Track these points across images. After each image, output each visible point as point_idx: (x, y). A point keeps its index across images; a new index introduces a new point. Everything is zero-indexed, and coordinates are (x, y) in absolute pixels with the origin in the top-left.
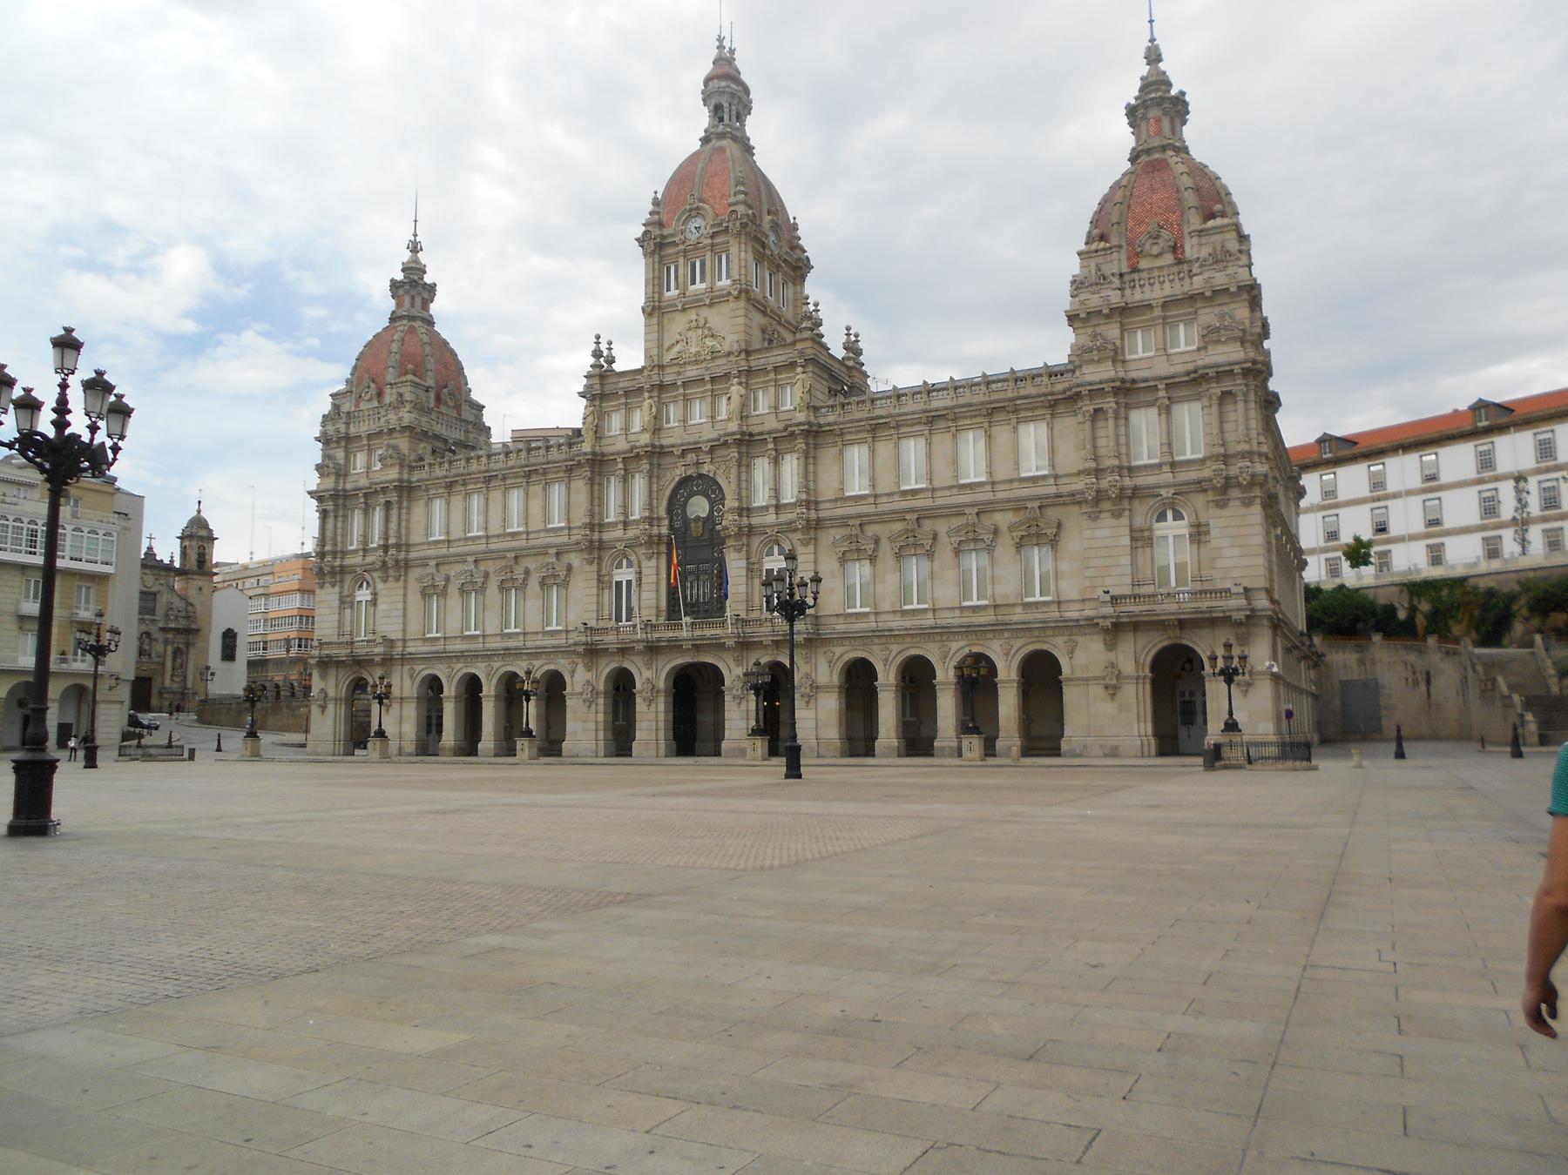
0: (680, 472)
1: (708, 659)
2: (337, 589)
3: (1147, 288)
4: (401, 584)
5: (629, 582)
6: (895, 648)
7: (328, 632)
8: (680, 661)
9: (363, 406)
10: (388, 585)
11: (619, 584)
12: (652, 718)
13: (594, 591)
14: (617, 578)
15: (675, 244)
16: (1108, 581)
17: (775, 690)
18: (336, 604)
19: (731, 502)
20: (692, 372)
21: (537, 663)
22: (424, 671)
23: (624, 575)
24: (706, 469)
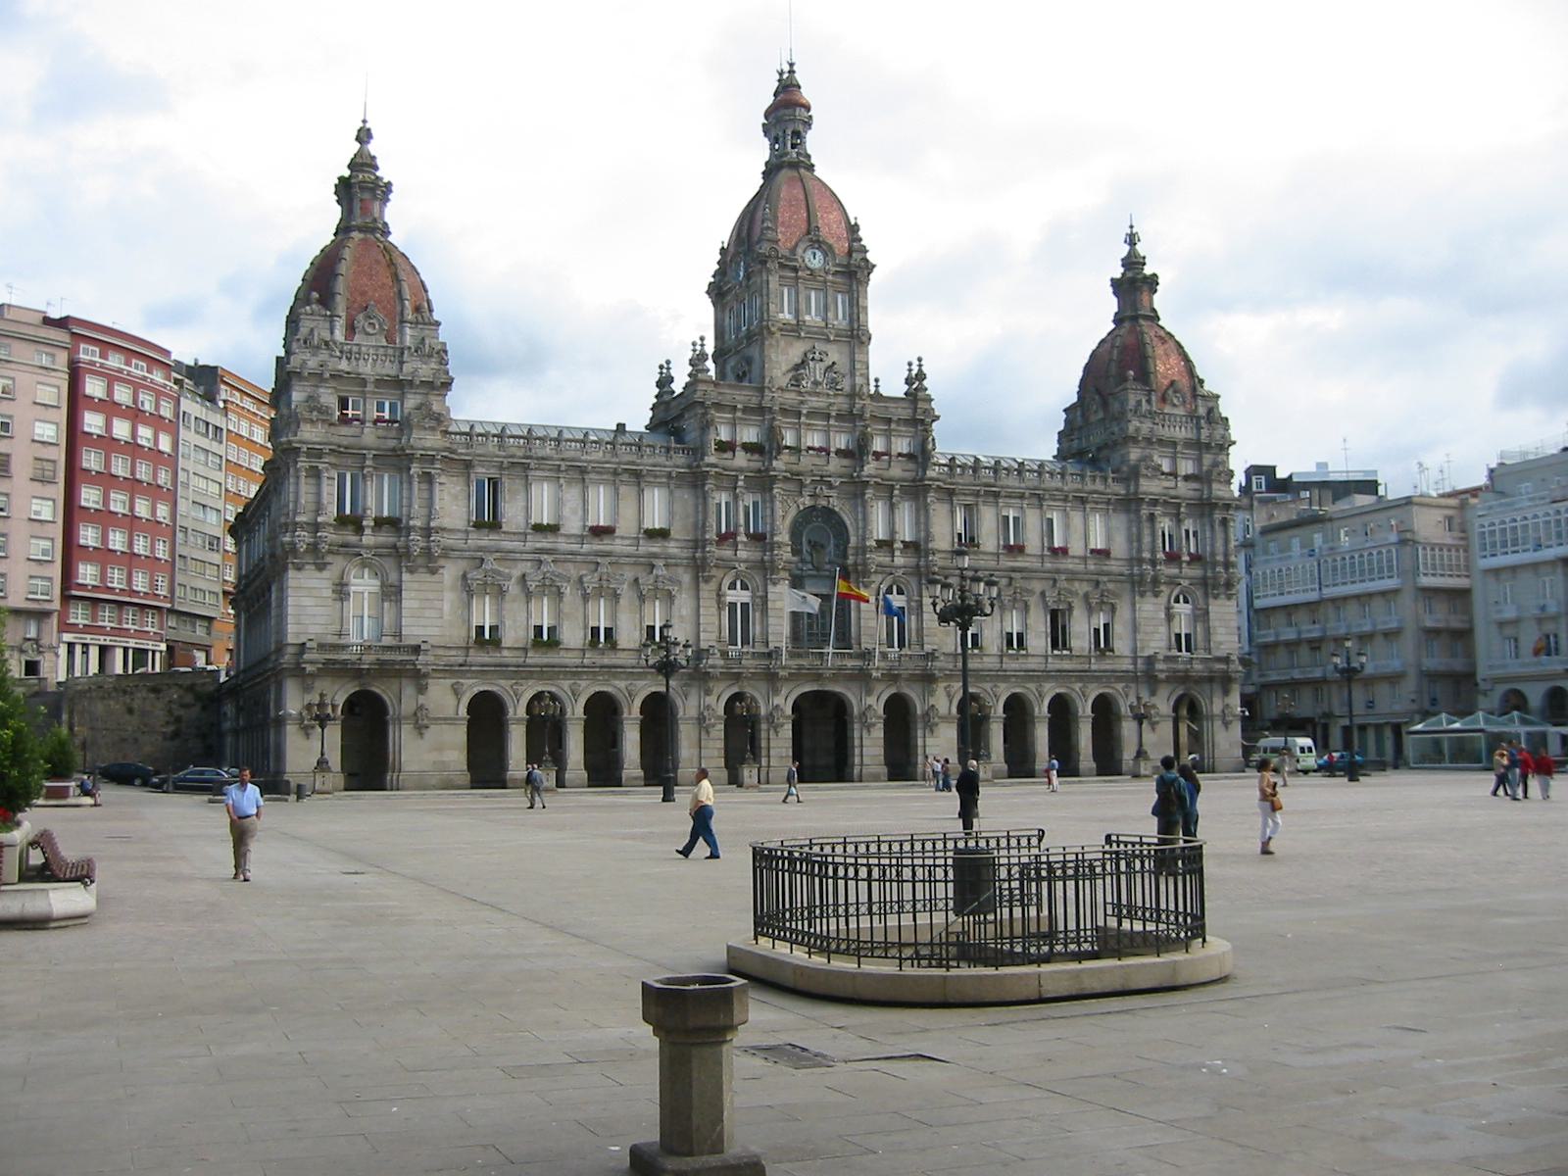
0: (808, 502)
1: (837, 688)
2: (326, 574)
3: (1172, 429)
4: (436, 577)
5: (745, 606)
6: (1002, 686)
7: (318, 630)
8: (807, 688)
9: (357, 339)
10: (416, 577)
11: (733, 606)
12: (779, 744)
13: (714, 610)
14: (729, 599)
15: (795, 270)
16: (1153, 644)
17: (900, 720)
18: (328, 593)
19: (853, 540)
20: (815, 402)
21: (583, 684)
22: (473, 687)
23: (739, 596)
24: (836, 504)
